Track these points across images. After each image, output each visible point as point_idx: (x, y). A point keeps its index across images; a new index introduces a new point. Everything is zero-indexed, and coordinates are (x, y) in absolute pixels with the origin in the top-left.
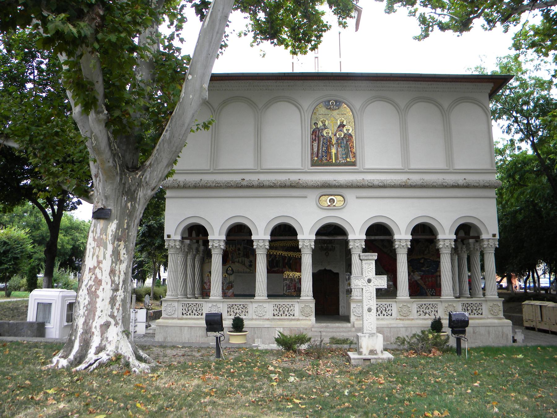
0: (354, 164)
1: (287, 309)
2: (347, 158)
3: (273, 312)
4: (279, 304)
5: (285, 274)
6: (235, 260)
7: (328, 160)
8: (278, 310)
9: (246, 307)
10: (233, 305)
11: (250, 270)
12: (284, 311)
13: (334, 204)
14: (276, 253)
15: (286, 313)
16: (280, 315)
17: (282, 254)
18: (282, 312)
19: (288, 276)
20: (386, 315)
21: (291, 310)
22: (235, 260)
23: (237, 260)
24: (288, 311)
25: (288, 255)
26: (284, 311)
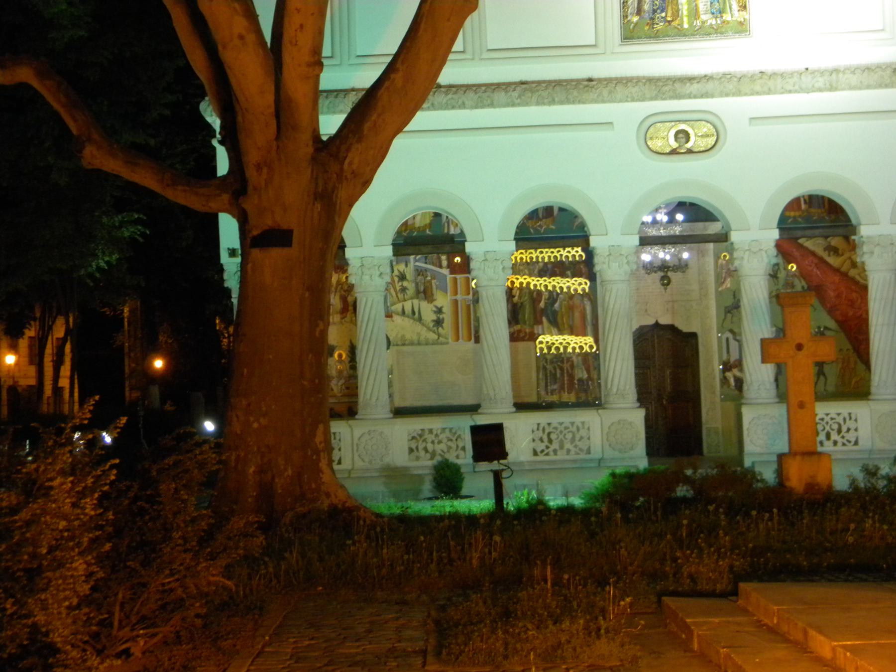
0: (742, 28)
1: (569, 436)
2: (721, 12)
3: (532, 445)
5: (541, 343)
6: (393, 308)
7: (669, 22)
8: (545, 438)
9: (459, 437)
10: (423, 430)
11: (439, 335)
13: (689, 145)
14: (513, 283)
15: (568, 445)
16: (552, 453)
17: (528, 284)
18: (555, 445)
19: (549, 348)
20: (840, 444)
21: (581, 438)
22: (393, 308)
23: (398, 307)
24: (573, 440)
25: (546, 286)
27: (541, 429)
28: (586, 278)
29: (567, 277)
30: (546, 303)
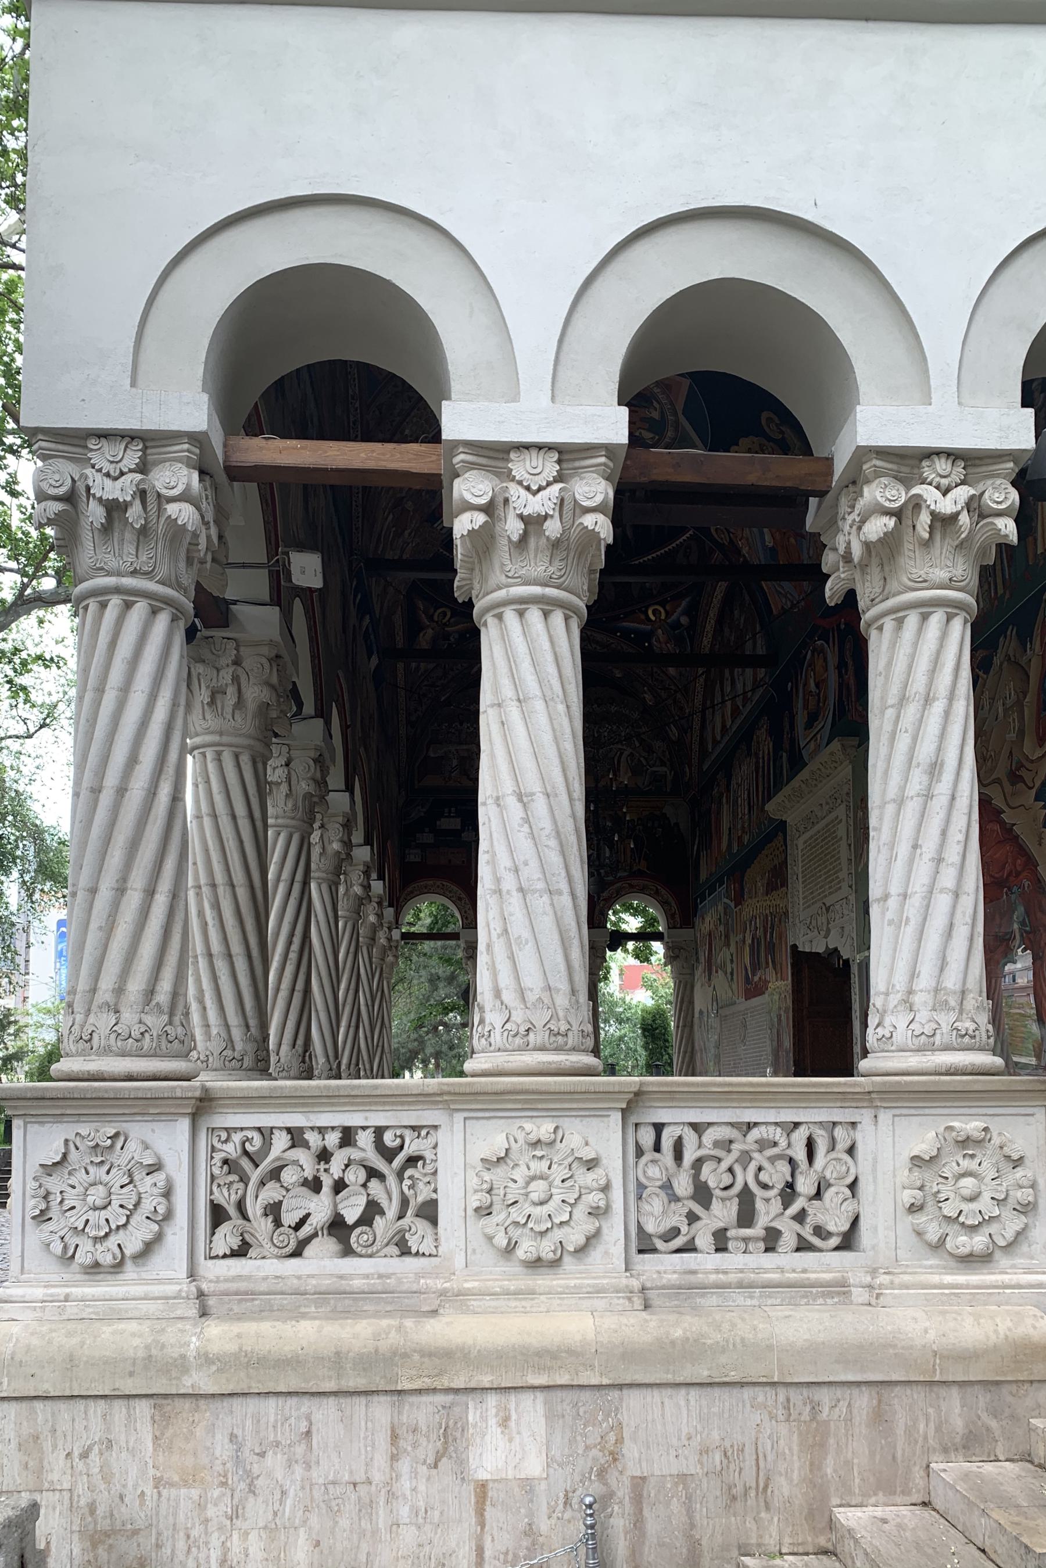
1: (777, 1175)
4: (698, 1128)
8: (683, 1185)
12: (746, 1198)
24: (789, 1191)
26: (746, 1198)
27: (667, 1143)
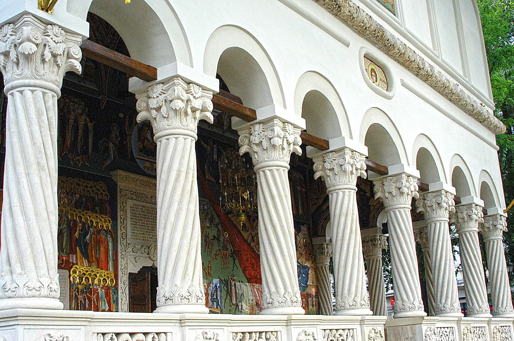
28: (110, 217)
29: (96, 212)
30: (80, 234)
